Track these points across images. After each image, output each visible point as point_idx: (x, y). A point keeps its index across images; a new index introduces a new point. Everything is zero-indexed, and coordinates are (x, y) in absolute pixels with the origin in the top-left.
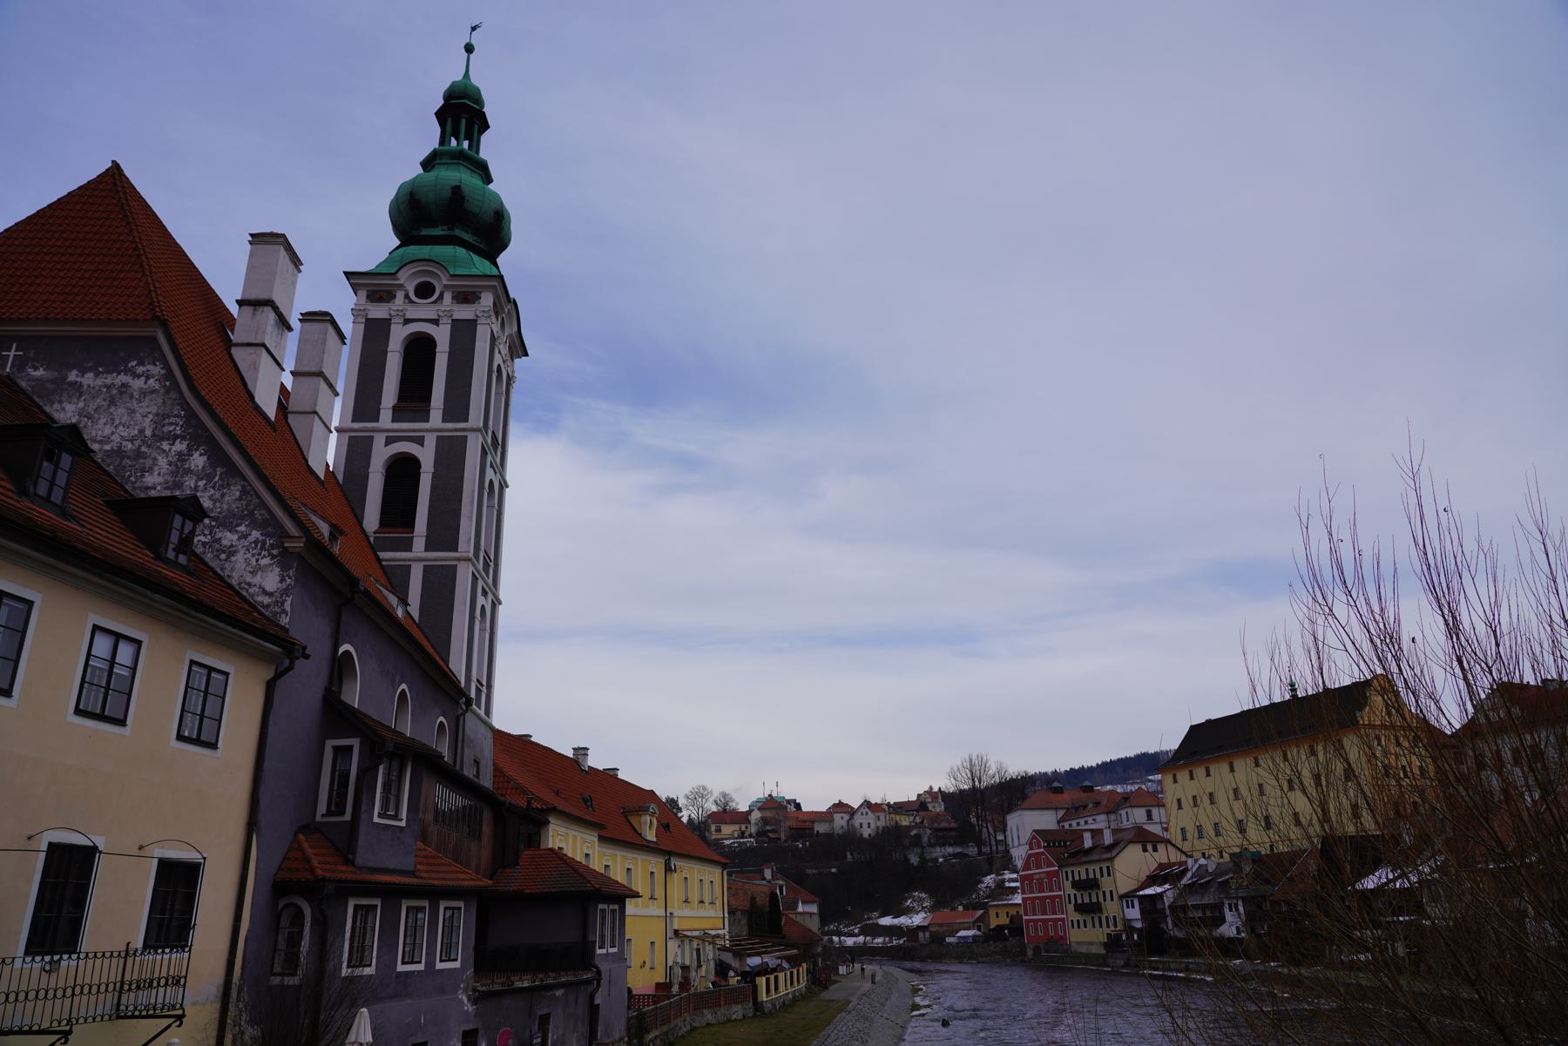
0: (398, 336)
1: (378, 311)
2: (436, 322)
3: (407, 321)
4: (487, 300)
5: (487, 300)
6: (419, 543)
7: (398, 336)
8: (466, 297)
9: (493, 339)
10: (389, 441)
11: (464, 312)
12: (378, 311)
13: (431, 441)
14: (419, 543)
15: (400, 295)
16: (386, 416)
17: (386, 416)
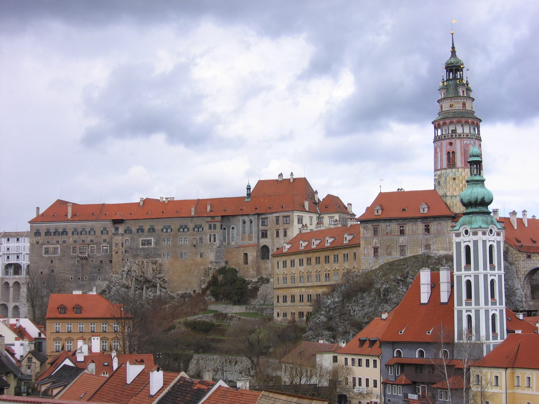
0: (463, 246)
1: (458, 239)
2: (469, 241)
3: (464, 242)
4: (480, 233)
5: (480, 233)
6: (473, 304)
7: (463, 246)
8: (475, 234)
9: (484, 242)
10: (465, 276)
11: (475, 238)
12: (458, 239)
13: (473, 276)
14: (473, 304)
15: (462, 234)
16: (463, 269)
17: (463, 269)
